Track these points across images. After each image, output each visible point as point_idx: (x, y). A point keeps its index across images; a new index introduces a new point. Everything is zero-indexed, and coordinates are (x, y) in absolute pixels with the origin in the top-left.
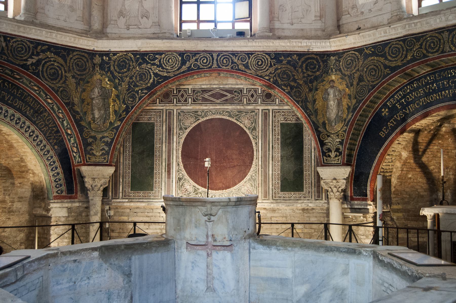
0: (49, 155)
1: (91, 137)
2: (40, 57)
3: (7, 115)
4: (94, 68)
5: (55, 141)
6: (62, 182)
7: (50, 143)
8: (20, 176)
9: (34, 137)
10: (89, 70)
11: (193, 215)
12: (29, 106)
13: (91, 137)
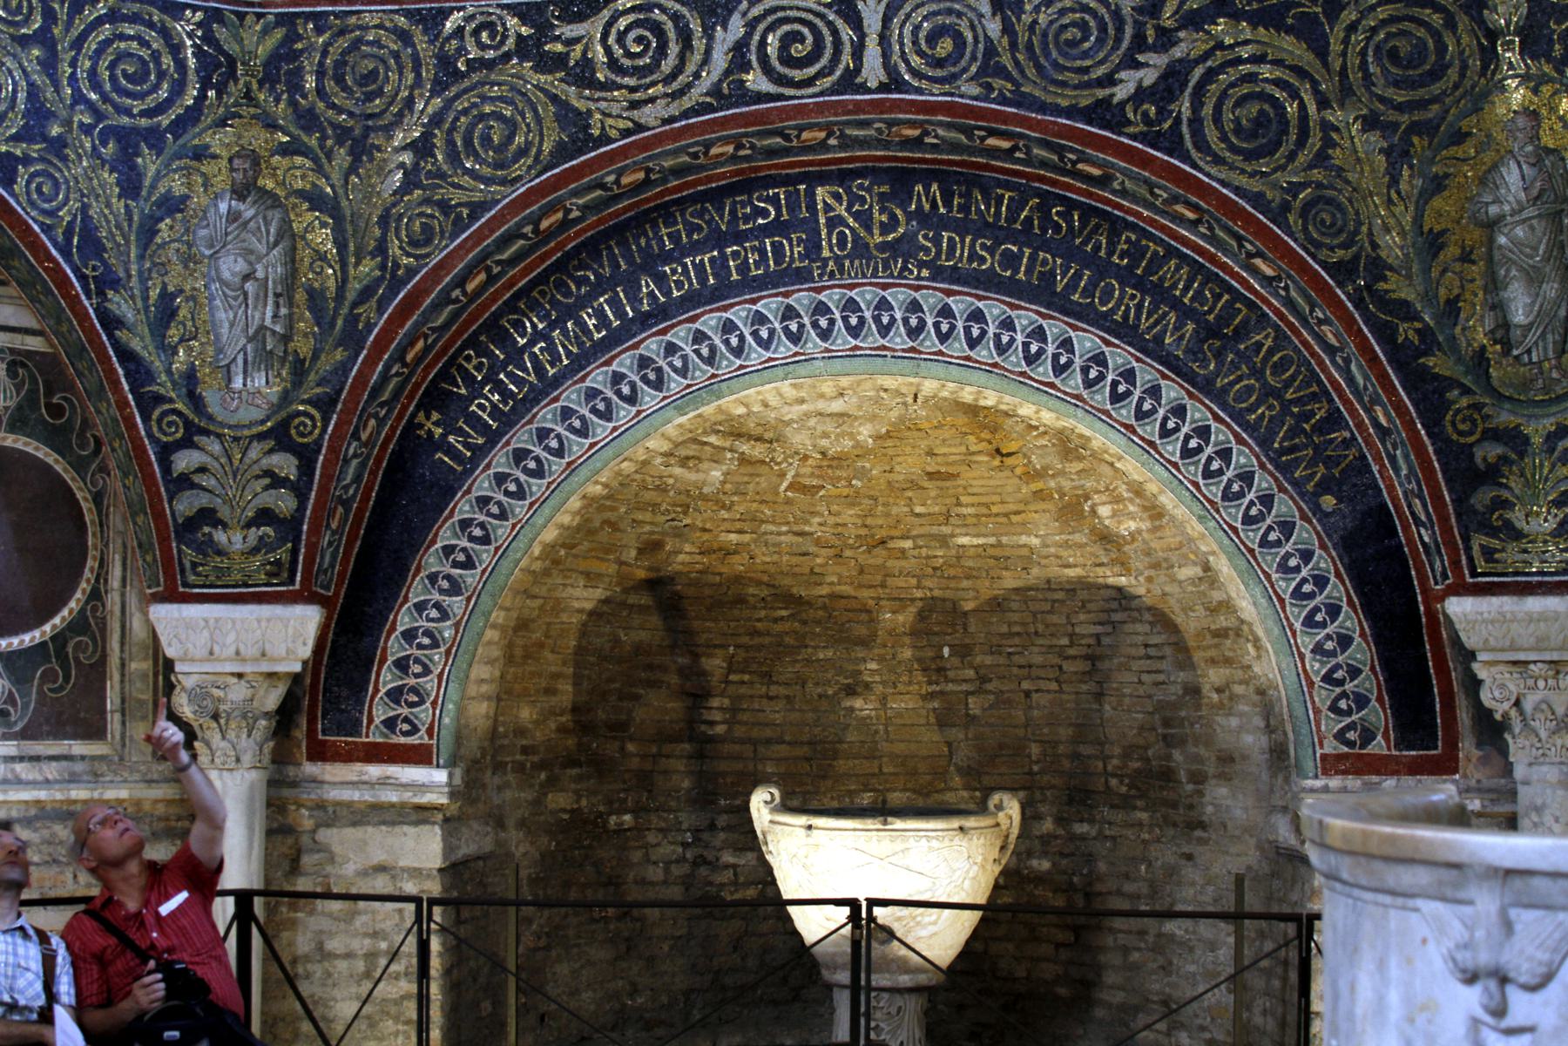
0: (1288, 547)
1: (1494, 435)
2: (1178, 52)
3: (1070, 363)
4: (1489, 56)
5: (1321, 470)
6: (1367, 683)
7: (1296, 484)
8: (1212, 653)
9: (1210, 460)
10: (1464, 67)
11: (1394, 971)
12: (1176, 304)
13: (1494, 435)
